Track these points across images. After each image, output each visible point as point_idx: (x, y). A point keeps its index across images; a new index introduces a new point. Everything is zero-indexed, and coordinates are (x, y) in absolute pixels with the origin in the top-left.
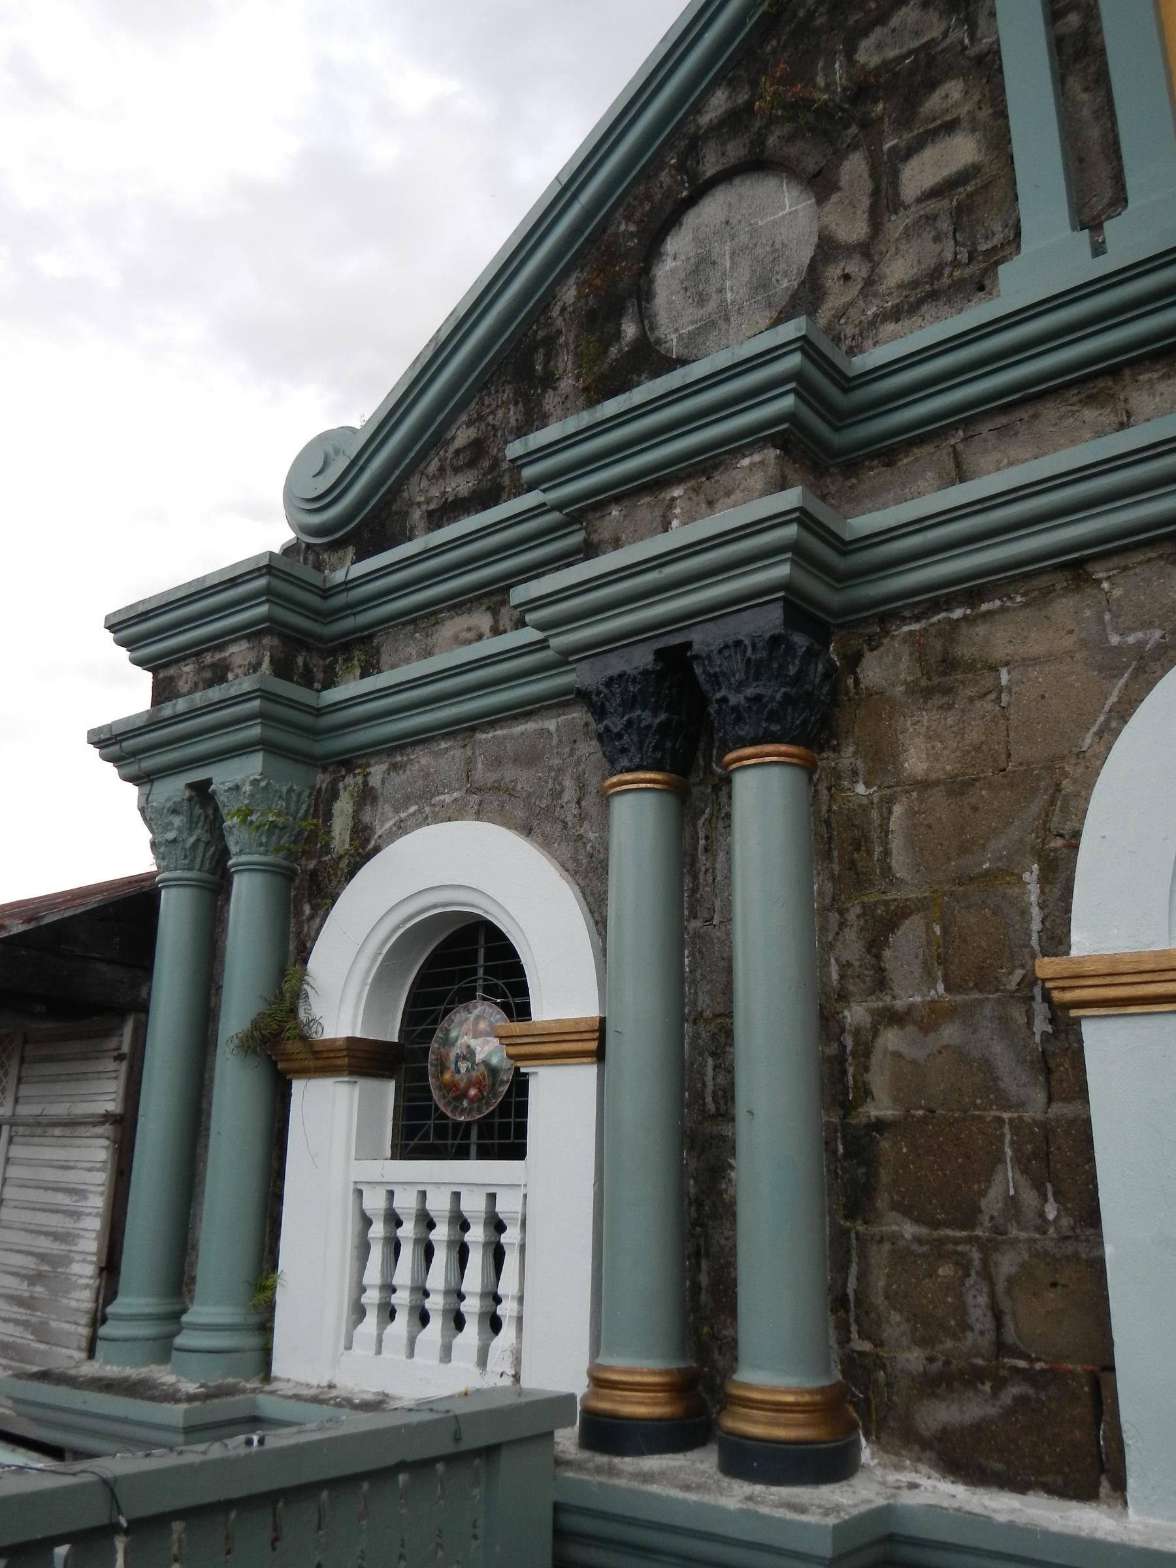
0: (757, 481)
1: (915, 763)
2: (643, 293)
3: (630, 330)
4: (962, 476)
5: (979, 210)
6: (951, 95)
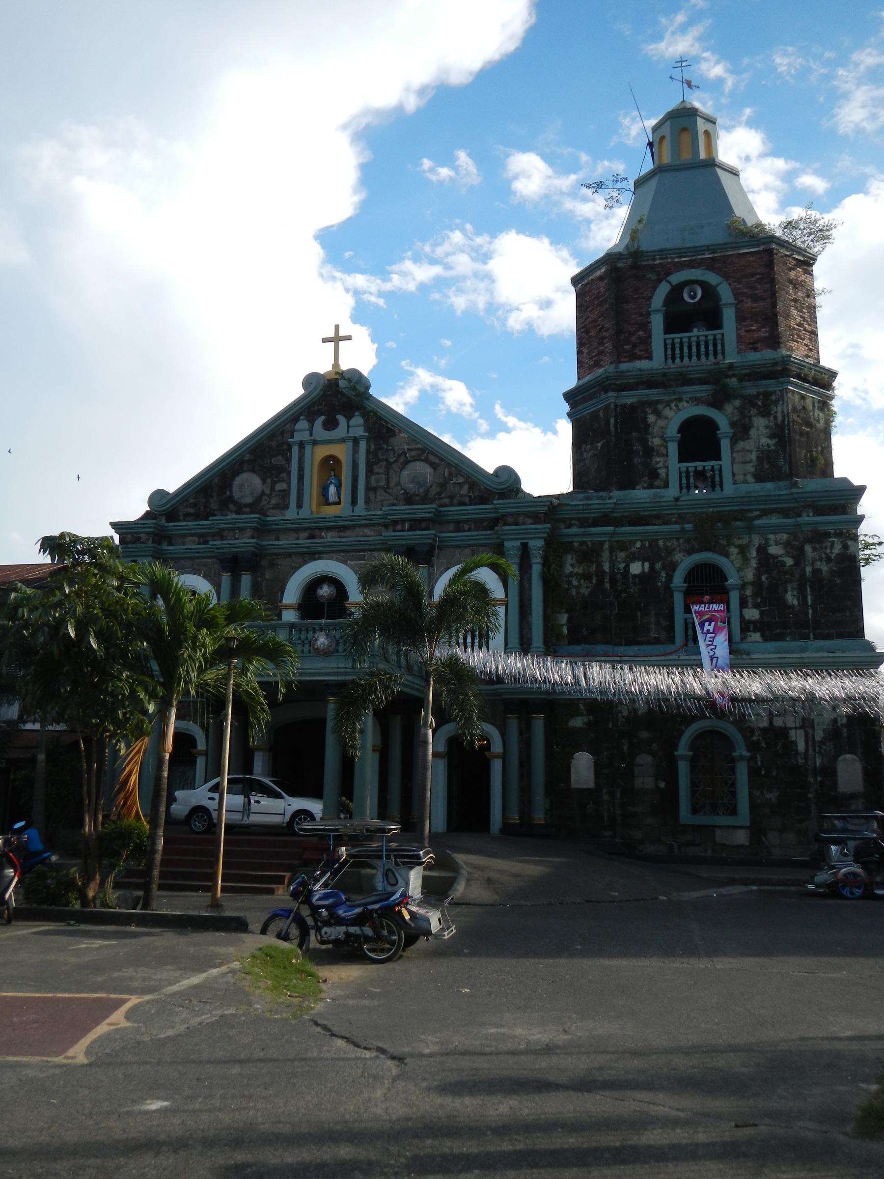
0: (250, 534)
1: (267, 577)
2: (230, 486)
3: (228, 493)
4: (278, 539)
5: (285, 494)
6: (284, 475)
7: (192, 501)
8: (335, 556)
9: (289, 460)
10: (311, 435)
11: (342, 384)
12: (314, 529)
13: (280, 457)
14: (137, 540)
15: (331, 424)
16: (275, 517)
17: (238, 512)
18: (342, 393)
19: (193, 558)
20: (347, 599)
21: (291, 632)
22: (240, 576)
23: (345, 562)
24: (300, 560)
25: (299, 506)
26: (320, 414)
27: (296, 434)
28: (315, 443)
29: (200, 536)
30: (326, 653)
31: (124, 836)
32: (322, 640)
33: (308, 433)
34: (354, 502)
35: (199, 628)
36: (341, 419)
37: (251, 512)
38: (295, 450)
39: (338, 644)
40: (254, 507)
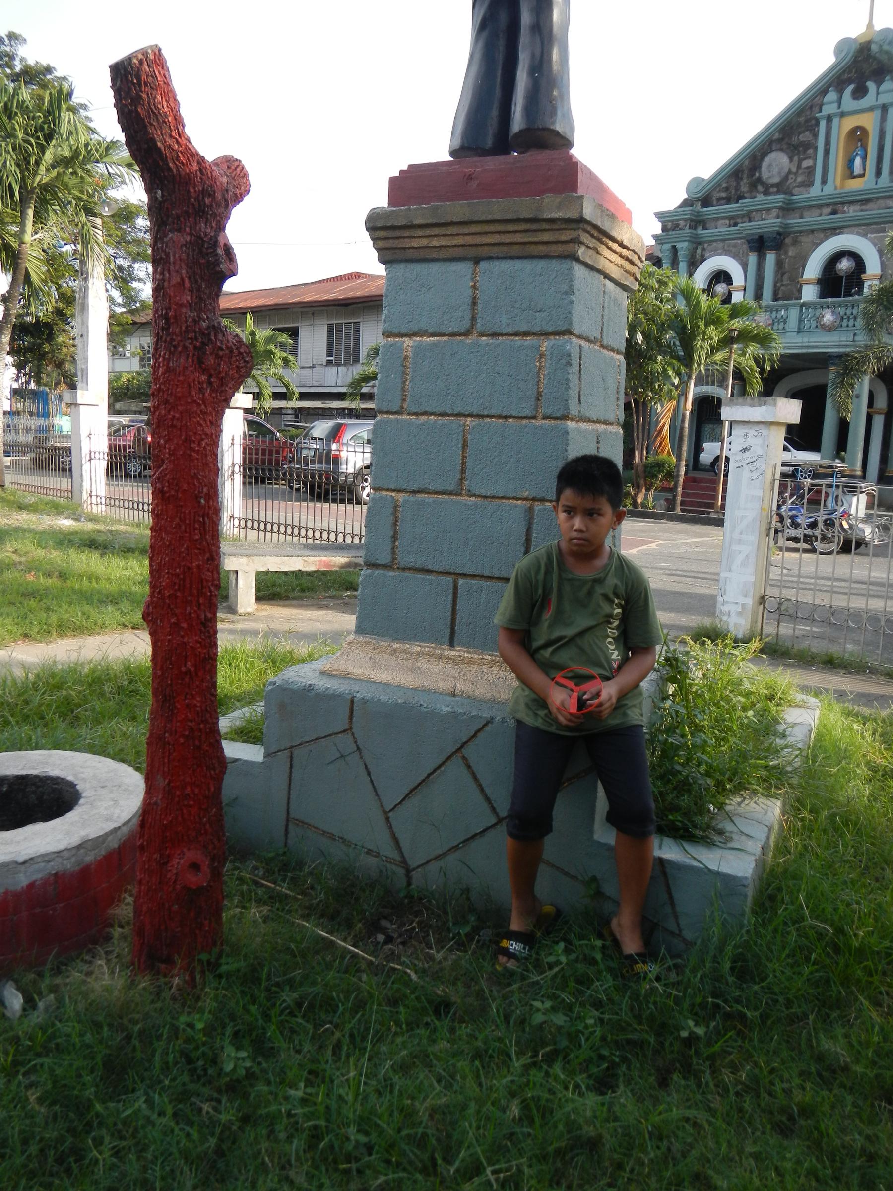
1: (790, 254)
2: (760, 167)
4: (801, 217)
5: (811, 170)
6: (811, 151)
7: (724, 185)
8: (856, 230)
9: (816, 136)
10: (839, 107)
11: (874, 47)
12: (836, 205)
13: (807, 133)
14: (676, 227)
15: (860, 92)
16: (802, 196)
17: (766, 193)
18: (875, 58)
19: (723, 240)
20: (865, 273)
21: (801, 310)
22: (765, 254)
23: (865, 235)
24: (822, 235)
25: (824, 182)
26: (850, 81)
27: (824, 107)
28: (843, 115)
29: (730, 218)
30: (830, 329)
31: (660, 465)
32: (828, 317)
33: (836, 105)
34: (878, 173)
35: (707, 325)
36: (871, 85)
37: (778, 192)
38: (823, 124)
39: (842, 319)
40: (781, 187)
